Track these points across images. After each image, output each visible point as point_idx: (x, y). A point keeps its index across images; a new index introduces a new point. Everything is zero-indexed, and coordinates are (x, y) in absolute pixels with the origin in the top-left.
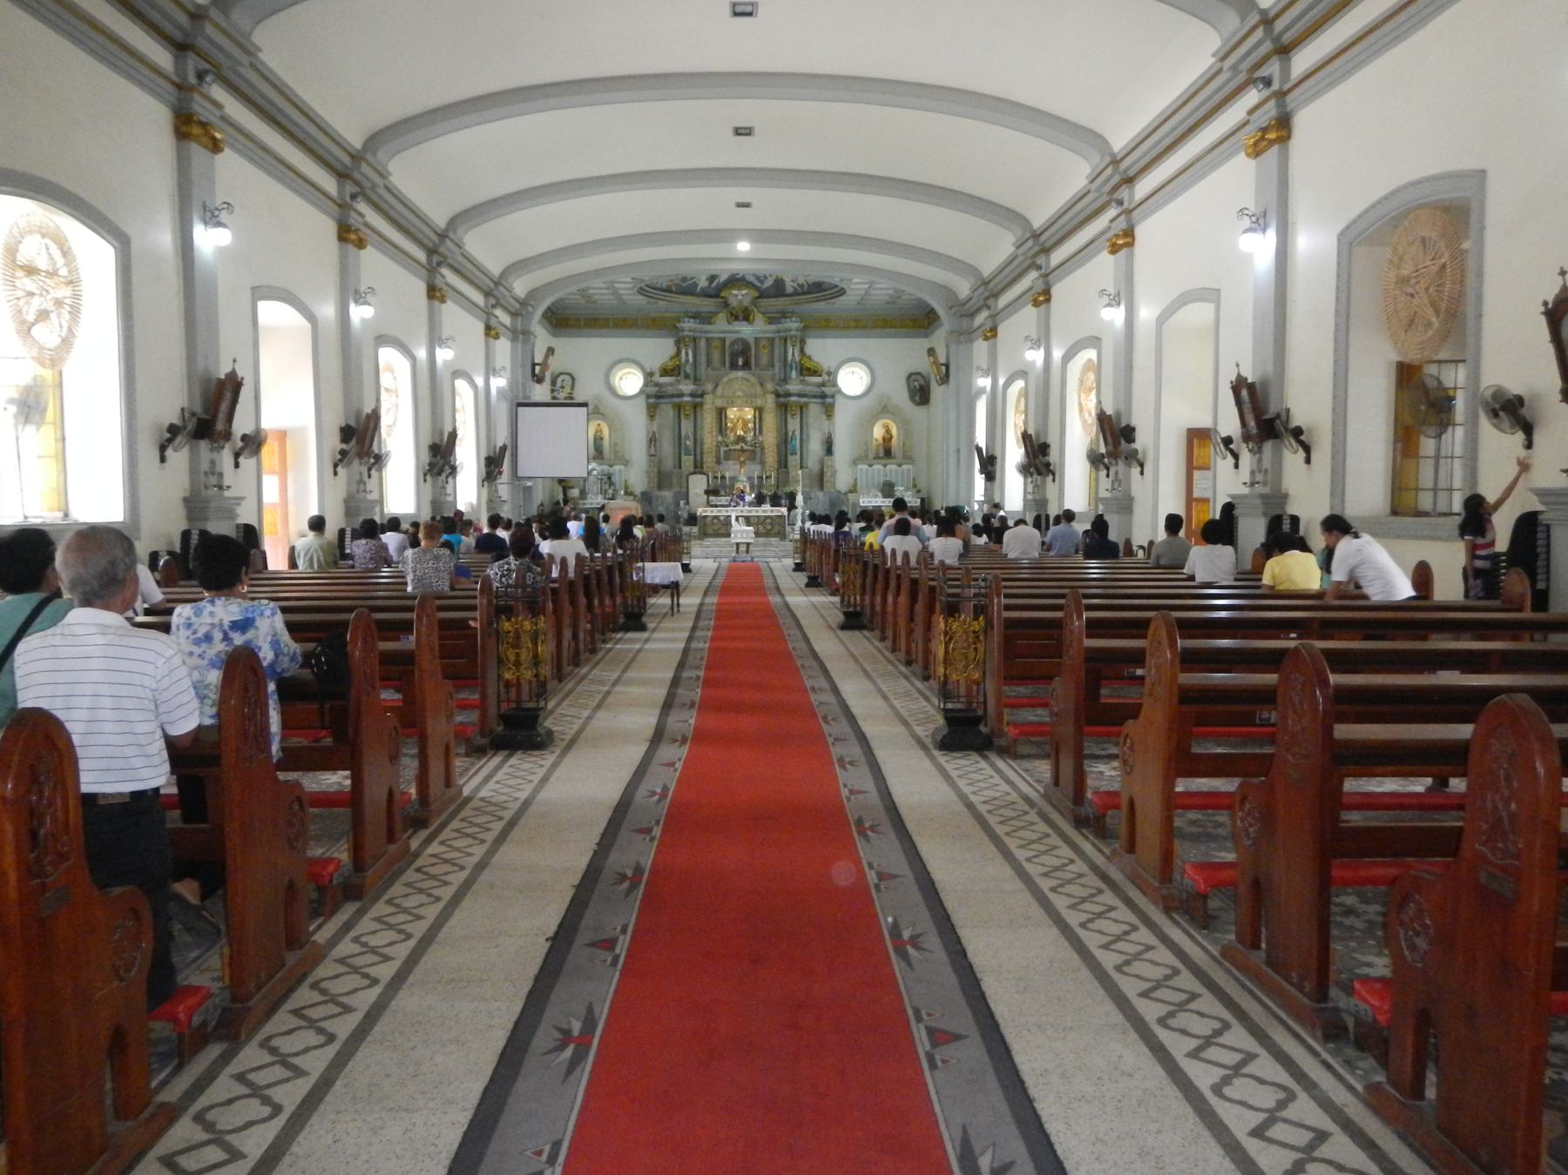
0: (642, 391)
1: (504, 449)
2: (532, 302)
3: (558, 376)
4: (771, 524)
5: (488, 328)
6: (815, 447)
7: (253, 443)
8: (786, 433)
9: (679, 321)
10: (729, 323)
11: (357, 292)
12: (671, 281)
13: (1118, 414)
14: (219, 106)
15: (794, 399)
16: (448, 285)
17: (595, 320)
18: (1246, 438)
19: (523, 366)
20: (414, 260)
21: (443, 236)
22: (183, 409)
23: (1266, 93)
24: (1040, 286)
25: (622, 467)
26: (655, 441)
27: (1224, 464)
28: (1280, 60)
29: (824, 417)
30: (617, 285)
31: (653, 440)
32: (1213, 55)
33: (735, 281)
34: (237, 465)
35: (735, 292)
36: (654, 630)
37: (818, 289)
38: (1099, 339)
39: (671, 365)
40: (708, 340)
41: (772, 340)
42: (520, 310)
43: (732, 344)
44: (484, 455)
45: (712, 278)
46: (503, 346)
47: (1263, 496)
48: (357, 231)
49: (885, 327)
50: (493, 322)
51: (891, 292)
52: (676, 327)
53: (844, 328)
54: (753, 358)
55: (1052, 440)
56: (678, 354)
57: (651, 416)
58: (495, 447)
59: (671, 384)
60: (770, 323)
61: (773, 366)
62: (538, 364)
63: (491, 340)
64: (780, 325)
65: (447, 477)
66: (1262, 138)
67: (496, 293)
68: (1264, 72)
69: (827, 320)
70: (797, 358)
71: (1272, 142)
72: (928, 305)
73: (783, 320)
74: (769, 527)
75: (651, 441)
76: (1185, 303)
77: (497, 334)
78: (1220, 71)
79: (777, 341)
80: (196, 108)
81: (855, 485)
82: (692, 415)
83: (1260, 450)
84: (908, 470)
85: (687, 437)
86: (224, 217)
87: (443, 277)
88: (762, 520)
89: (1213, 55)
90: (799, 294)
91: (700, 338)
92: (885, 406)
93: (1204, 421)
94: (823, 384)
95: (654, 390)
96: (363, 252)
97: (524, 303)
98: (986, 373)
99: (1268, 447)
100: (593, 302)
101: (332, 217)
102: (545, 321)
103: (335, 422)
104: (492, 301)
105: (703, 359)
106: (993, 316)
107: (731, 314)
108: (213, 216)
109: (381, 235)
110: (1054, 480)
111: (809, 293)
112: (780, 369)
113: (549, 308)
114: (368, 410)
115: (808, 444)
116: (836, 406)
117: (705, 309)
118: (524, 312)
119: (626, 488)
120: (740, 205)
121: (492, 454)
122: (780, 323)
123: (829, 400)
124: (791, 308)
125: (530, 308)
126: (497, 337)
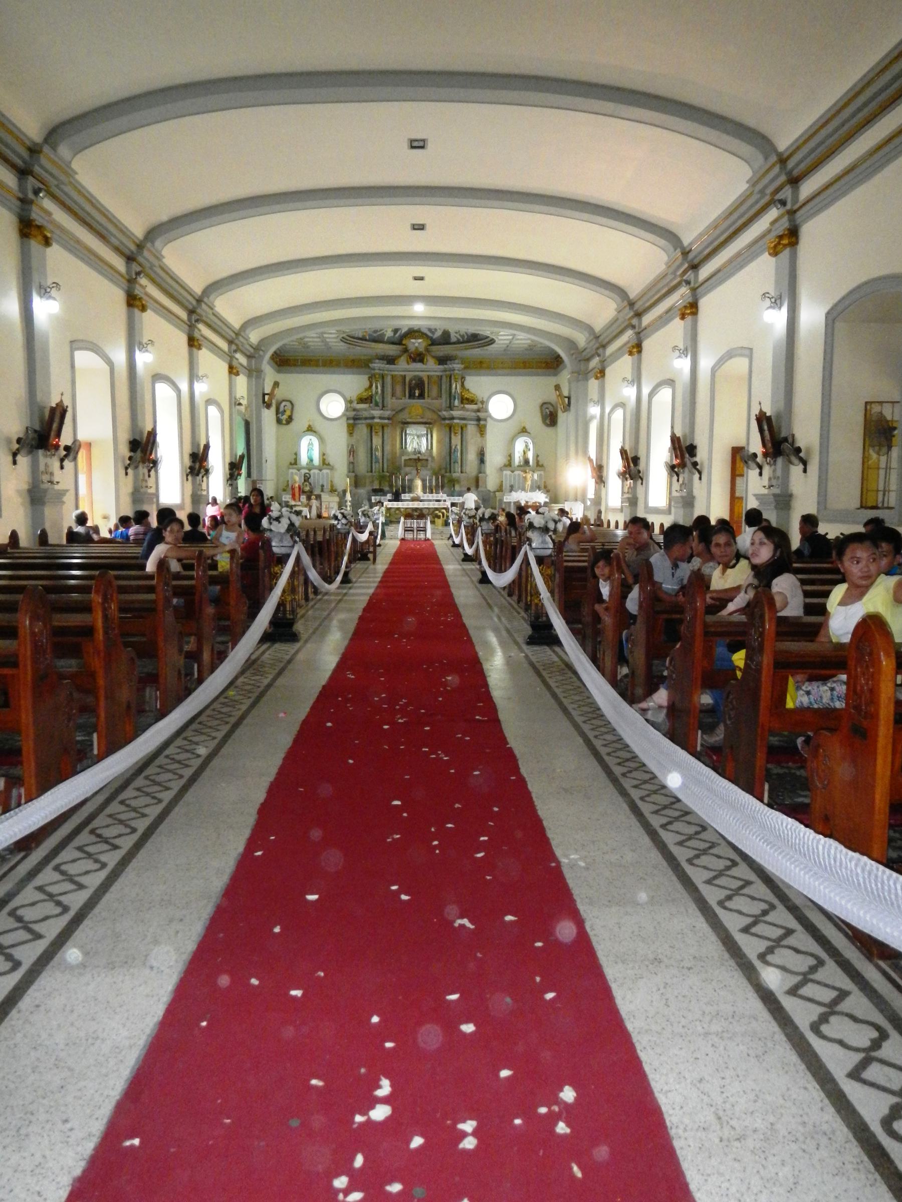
0: (344, 415)
1: (242, 457)
2: (263, 348)
3: (281, 403)
5: (231, 368)
6: (472, 456)
7: (71, 451)
8: (450, 447)
9: (370, 361)
10: (408, 363)
11: (140, 343)
12: (366, 332)
13: (685, 436)
14: (49, 214)
15: (456, 421)
16: (202, 336)
17: (310, 360)
18: (765, 455)
19: (256, 395)
20: (178, 318)
21: (199, 301)
22: (27, 428)
23: (783, 210)
24: (635, 341)
25: (328, 471)
26: (354, 452)
27: (753, 473)
28: (792, 187)
29: (479, 435)
30: (325, 335)
31: (352, 452)
32: (747, 182)
33: (413, 333)
34: (62, 467)
35: (413, 341)
36: (356, 582)
37: (474, 339)
38: (673, 381)
39: (365, 395)
40: (393, 377)
41: (440, 378)
42: (254, 354)
43: (411, 381)
44: (228, 461)
45: (396, 331)
46: (241, 382)
47: (775, 495)
48: (140, 299)
49: (525, 367)
50: (235, 363)
51: (529, 342)
52: (369, 367)
55: (642, 454)
56: (371, 386)
58: (236, 456)
59: (365, 410)
62: (267, 394)
63: (233, 376)
65: (203, 477)
66: (779, 243)
67: (236, 341)
68: (780, 196)
69: (481, 362)
70: (459, 390)
71: (785, 246)
72: (556, 352)
76: (731, 358)
77: (238, 372)
78: (751, 194)
79: (444, 379)
80: (34, 216)
81: (501, 486)
82: (380, 434)
83: (775, 461)
85: (377, 449)
86: (54, 292)
87: (200, 330)
88: (431, 510)
89: (747, 182)
91: (387, 375)
93: (742, 443)
94: (478, 411)
95: (352, 414)
96: (144, 314)
97: (257, 348)
98: (596, 403)
99: (780, 460)
100: (308, 347)
101: (123, 289)
102: (272, 361)
103: (124, 437)
104: (234, 347)
105: (389, 389)
106: (603, 362)
107: (410, 357)
108: (46, 292)
109: (156, 301)
110: (642, 484)
111: (468, 341)
113: (275, 352)
114: (149, 428)
116: (488, 427)
117: (391, 353)
118: (257, 355)
119: (332, 486)
120: (416, 279)
121: (234, 461)
122: (446, 364)
123: (482, 423)
124: (454, 353)
125: (261, 353)
126: (237, 374)
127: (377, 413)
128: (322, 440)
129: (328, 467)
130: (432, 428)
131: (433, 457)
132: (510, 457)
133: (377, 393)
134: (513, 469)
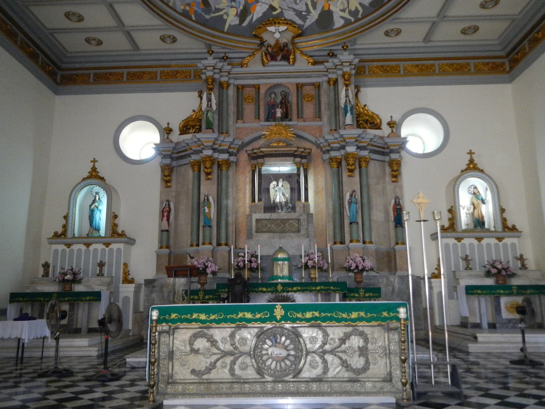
4: (363, 351)
10: (264, 66)
12: (188, 5)
25: (121, 246)
29: (388, 178)
35: (271, 29)
53: (405, 75)
54: (294, 108)
57: (167, 181)
60: (315, 63)
61: (320, 117)
64: (329, 65)
73: (330, 60)
74: (358, 362)
75: (163, 212)
79: (325, 86)
82: (214, 176)
84: (513, 245)
90: (352, 23)
92: (471, 161)
105: (232, 108)
112: (329, 118)
115: (370, 208)
119: (126, 273)
122: (327, 62)
123: (394, 156)
127: (206, 137)
128: (110, 191)
129: (123, 239)
130: (308, 164)
131: (310, 216)
132: (453, 211)
133: (209, 106)
134: (460, 235)
